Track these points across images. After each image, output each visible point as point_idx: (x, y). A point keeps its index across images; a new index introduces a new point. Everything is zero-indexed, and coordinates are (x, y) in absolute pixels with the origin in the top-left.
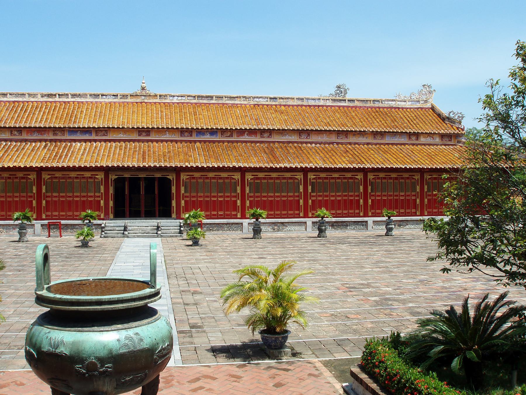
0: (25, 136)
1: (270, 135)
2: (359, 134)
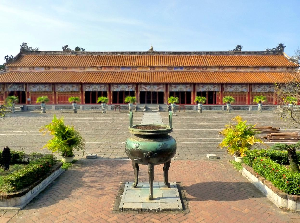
0: (103, 70)
1: (206, 68)
2: (246, 68)
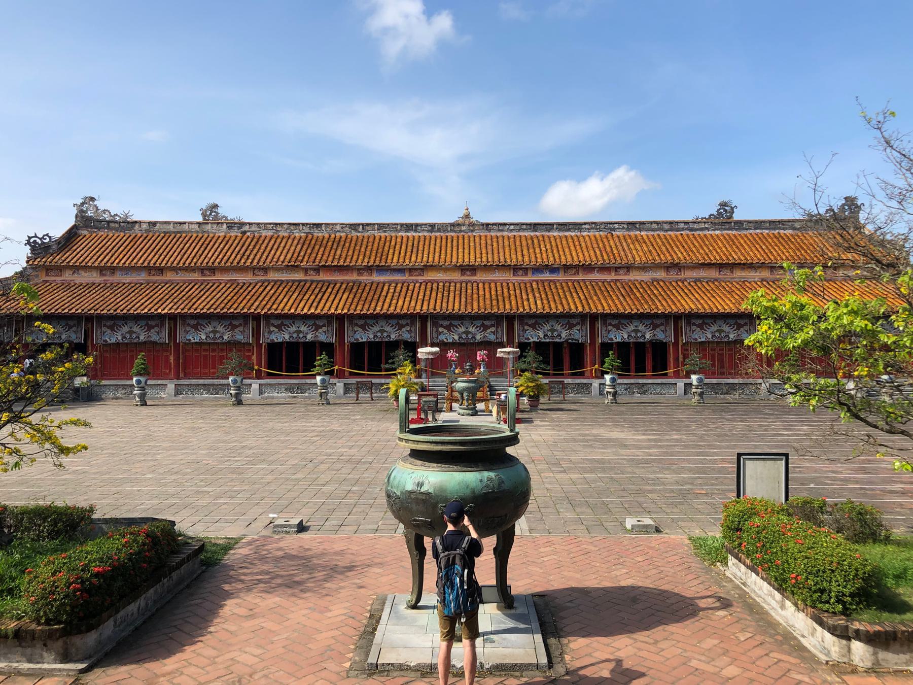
0: (323, 276)
1: (628, 271)
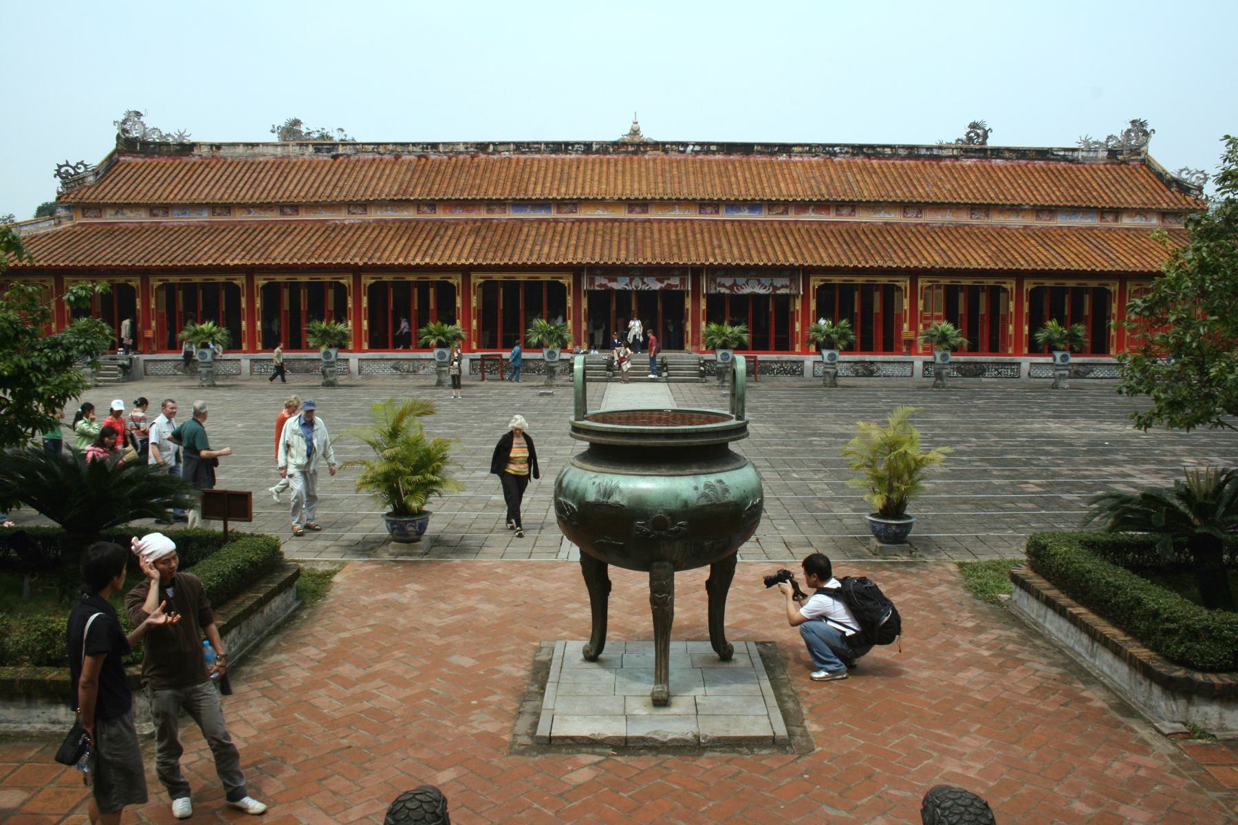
0: (441, 215)
1: (853, 211)
